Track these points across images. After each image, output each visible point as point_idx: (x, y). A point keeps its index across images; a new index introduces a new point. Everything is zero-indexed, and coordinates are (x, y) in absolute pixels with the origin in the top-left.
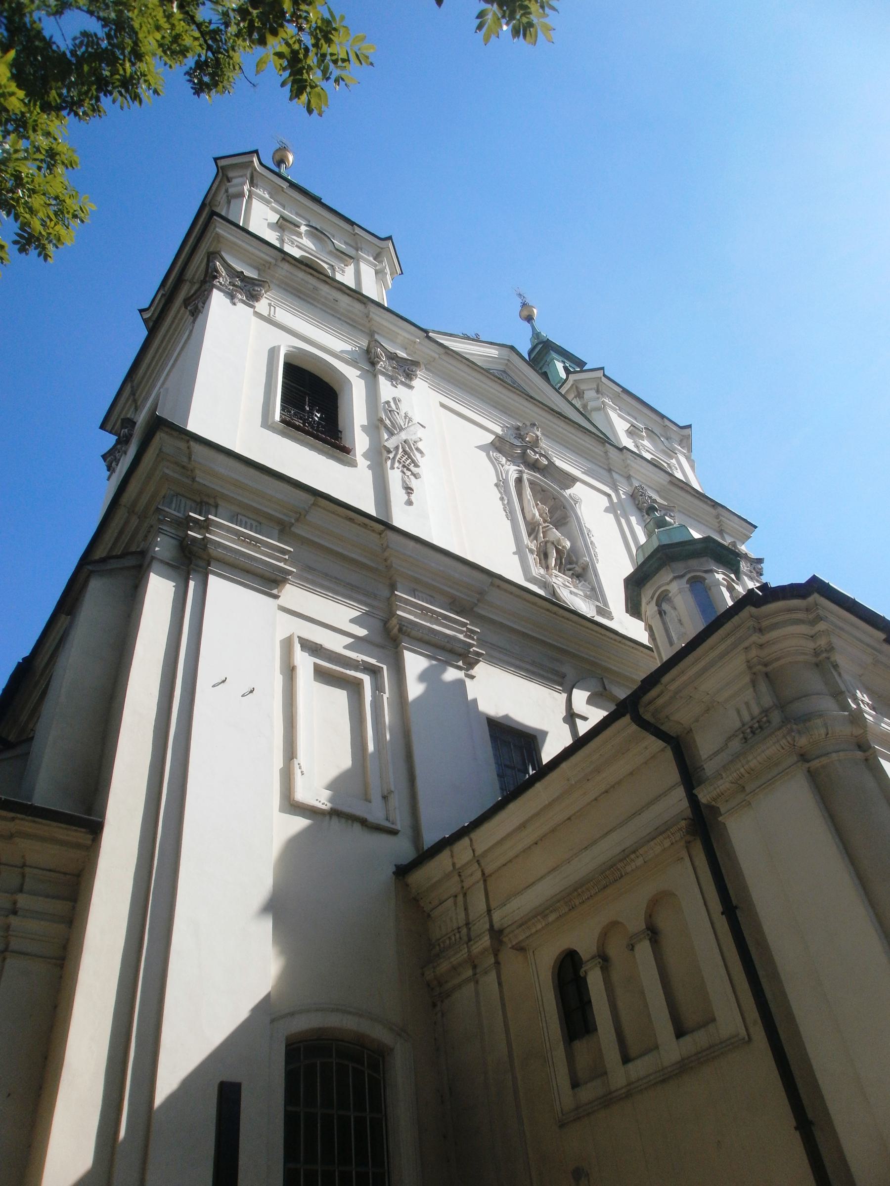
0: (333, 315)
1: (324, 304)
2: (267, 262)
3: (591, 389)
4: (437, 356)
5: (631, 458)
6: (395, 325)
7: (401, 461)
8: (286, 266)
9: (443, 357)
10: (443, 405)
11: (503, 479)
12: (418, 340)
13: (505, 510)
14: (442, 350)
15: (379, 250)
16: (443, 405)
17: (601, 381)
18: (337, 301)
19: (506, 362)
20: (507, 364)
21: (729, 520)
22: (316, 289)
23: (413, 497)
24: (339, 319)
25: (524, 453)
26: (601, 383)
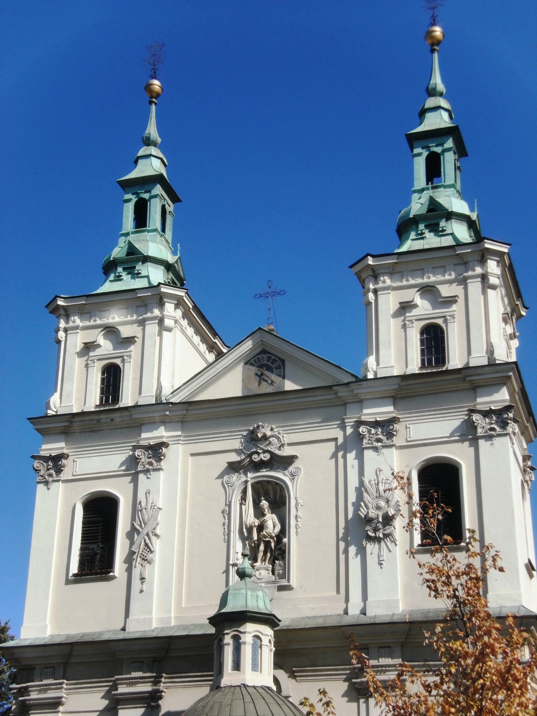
0: (116, 429)
1: (108, 426)
2: (65, 426)
3: (368, 277)
4: (185, 412)
5: (356, 387)
6: (150, 412)
7: (142, 556)
8: (77, 419)
9: (190, 408)
10: (193, 455)
11: (229, 502)
12: (168, 413)
13: (224, 535)
14: (185, 407)
15: (159, 296)
16: (193, 455)
17: (372, 265)
18: (112, 420)
19: (260, 343)
20: (262, 344)
21: (479, 375)
22: (99, 421)
23: (145, 587)
24: (120, 428)
25: (252, 461)
26: (373, 267)
